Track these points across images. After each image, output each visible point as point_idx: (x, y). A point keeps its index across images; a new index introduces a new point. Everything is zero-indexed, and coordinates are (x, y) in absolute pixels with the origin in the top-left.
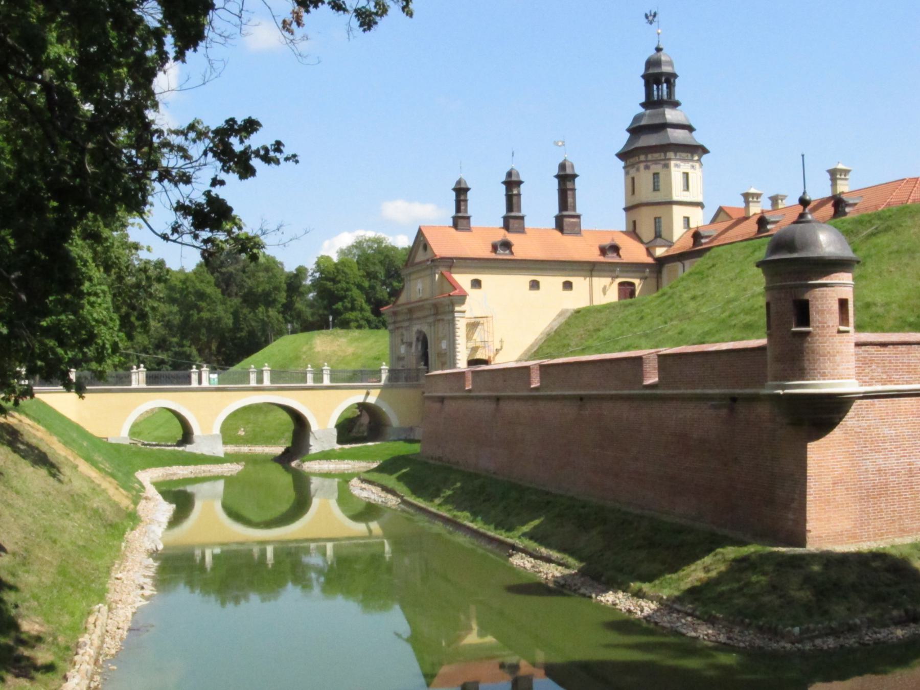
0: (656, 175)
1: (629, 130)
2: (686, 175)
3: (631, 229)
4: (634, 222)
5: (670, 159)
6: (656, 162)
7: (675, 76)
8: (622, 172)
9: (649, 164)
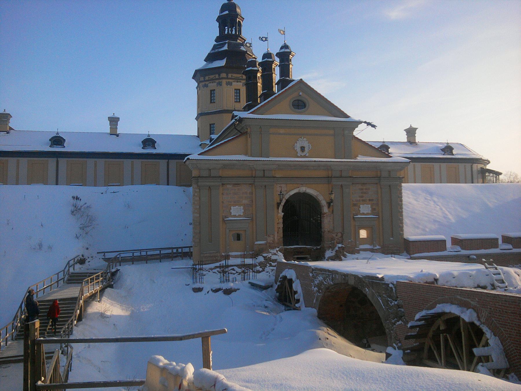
0: (212, 92)
9: (207, 83)
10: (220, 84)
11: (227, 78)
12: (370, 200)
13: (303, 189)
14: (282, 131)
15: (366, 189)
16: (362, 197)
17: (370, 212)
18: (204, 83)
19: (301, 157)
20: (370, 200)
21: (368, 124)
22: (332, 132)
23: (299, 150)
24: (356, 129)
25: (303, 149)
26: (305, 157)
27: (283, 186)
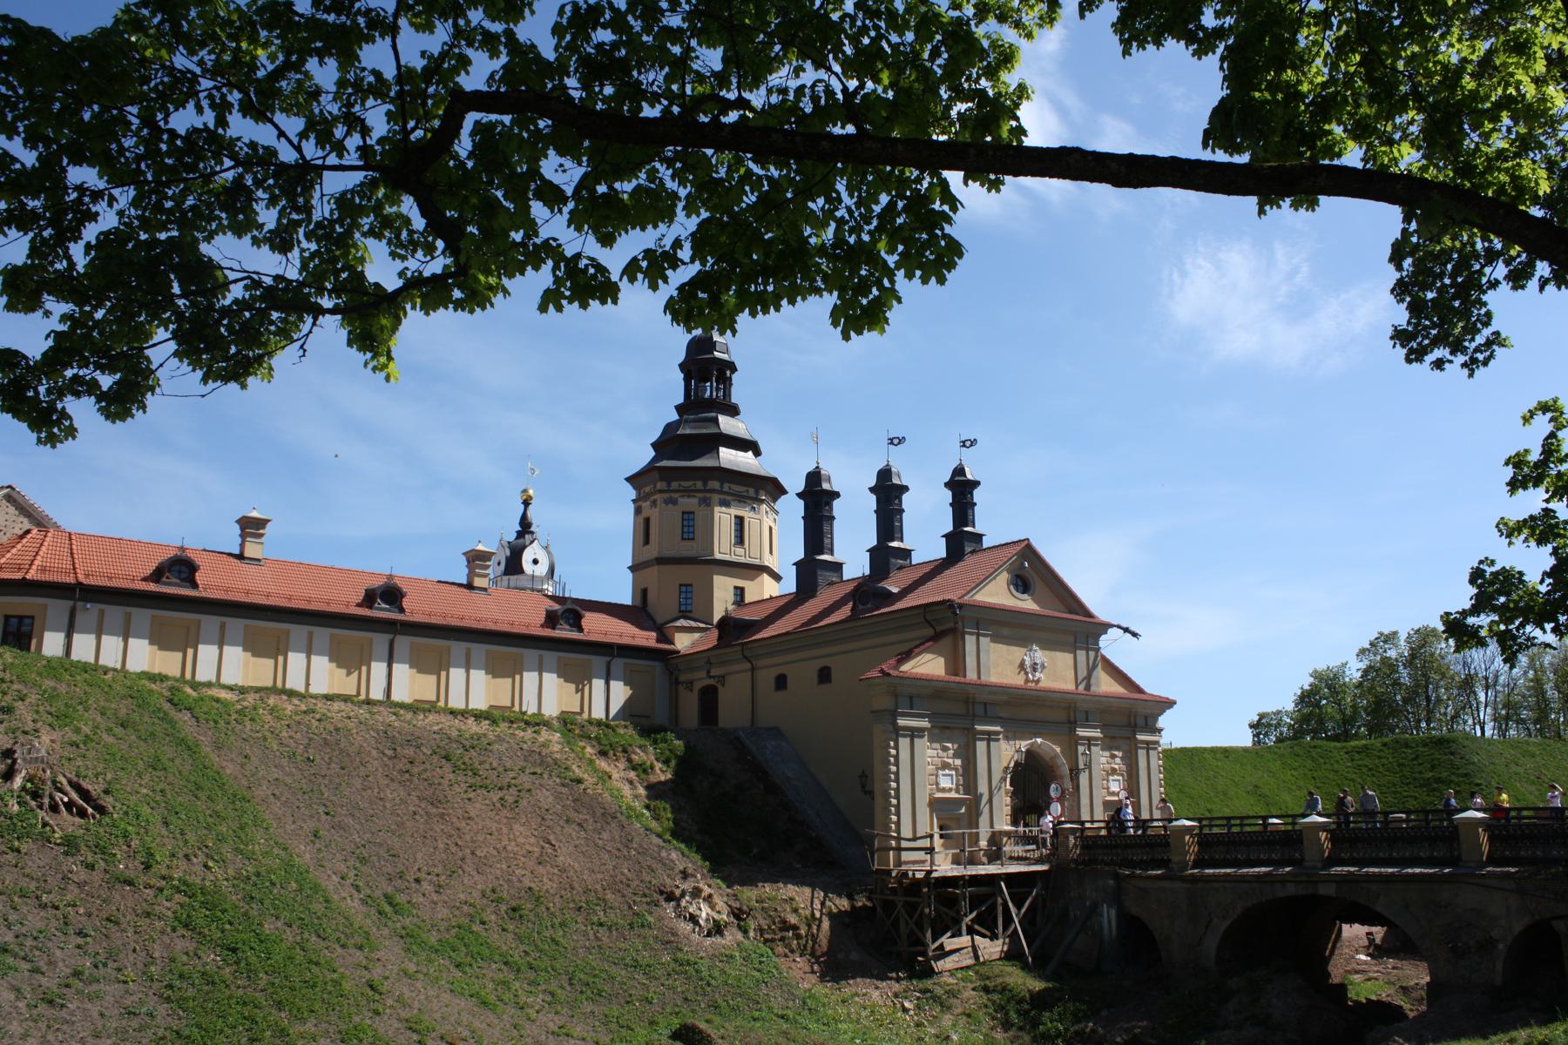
0: (688, 516)
1: (654, 445)
2: (740, 521)
3: (638, 603)
4: (645, 592)
5: (713, 491)
6: (688, 492)
7: (732, 367)
8: (631, 508)
10: (707, 503)
11: (721, 492)
18: (666, 496)
21: (1126, 630)
24: (1103, 637)
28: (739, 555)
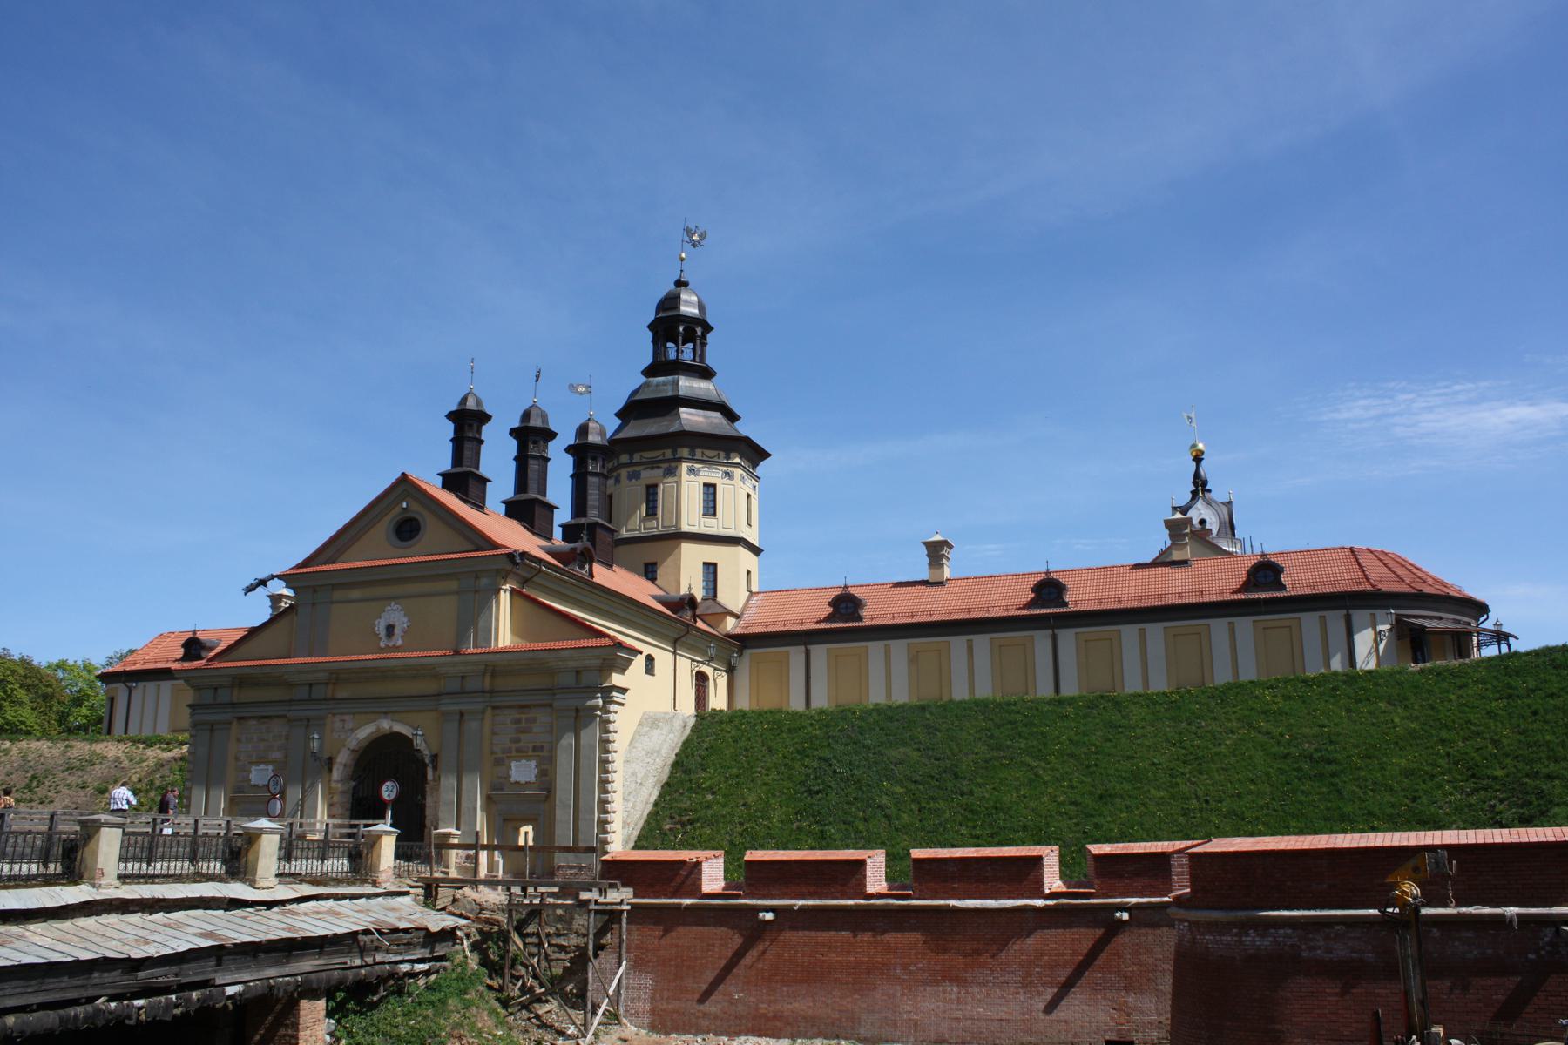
10: (618, 480)
12: (535, 749)
13: (386, 725)
14: (355, 594)
15: (527, 720)
16: (517, 741)
17: (533, 779)
19: (388, 649)
20: (535, 749)
22: (454, 585)
23: (383, 633)
25: (390, 629)
26: (396, 648)
27: (346, 717)
28: (657, 526)
